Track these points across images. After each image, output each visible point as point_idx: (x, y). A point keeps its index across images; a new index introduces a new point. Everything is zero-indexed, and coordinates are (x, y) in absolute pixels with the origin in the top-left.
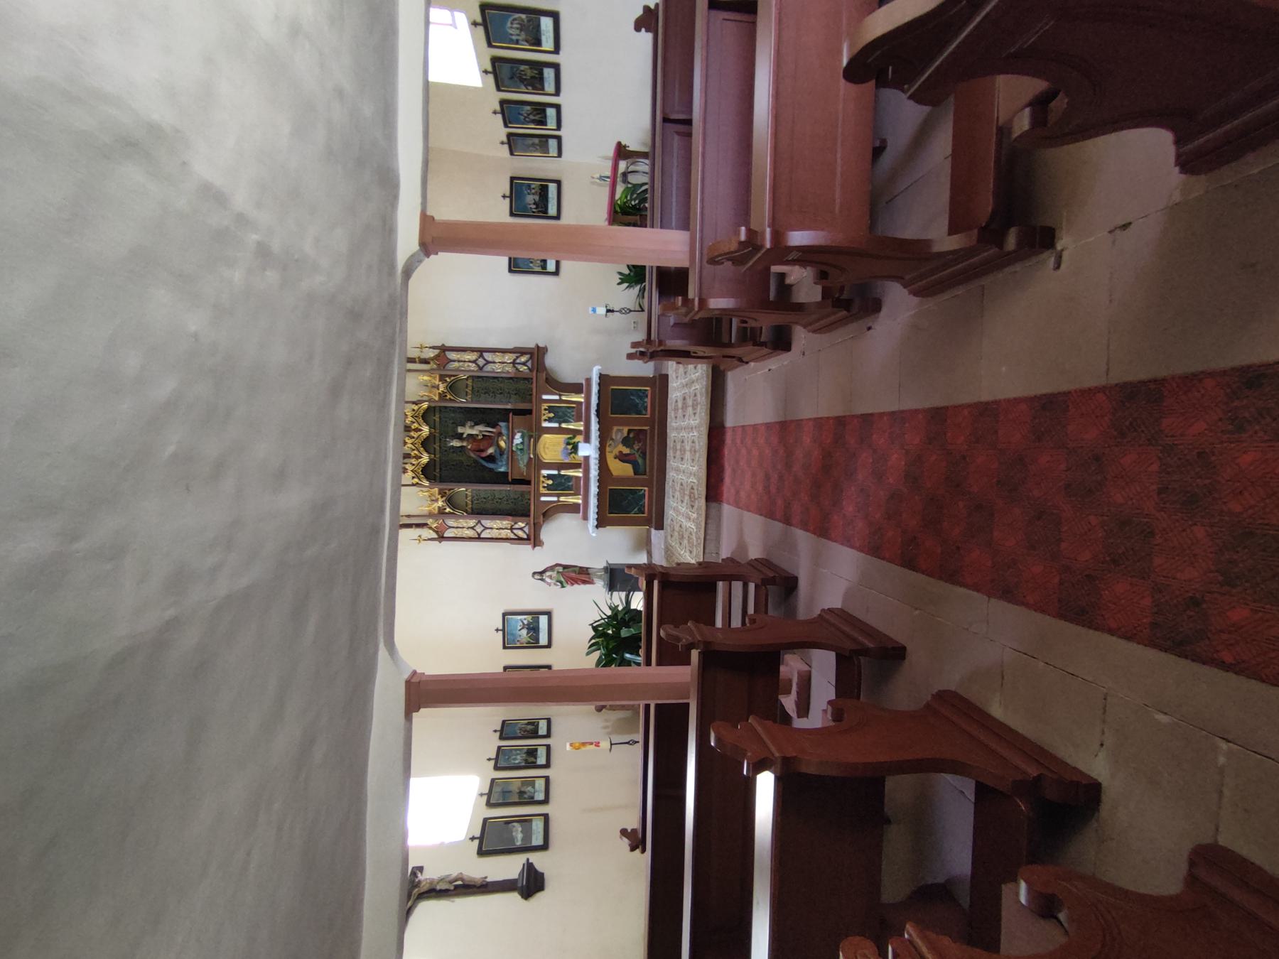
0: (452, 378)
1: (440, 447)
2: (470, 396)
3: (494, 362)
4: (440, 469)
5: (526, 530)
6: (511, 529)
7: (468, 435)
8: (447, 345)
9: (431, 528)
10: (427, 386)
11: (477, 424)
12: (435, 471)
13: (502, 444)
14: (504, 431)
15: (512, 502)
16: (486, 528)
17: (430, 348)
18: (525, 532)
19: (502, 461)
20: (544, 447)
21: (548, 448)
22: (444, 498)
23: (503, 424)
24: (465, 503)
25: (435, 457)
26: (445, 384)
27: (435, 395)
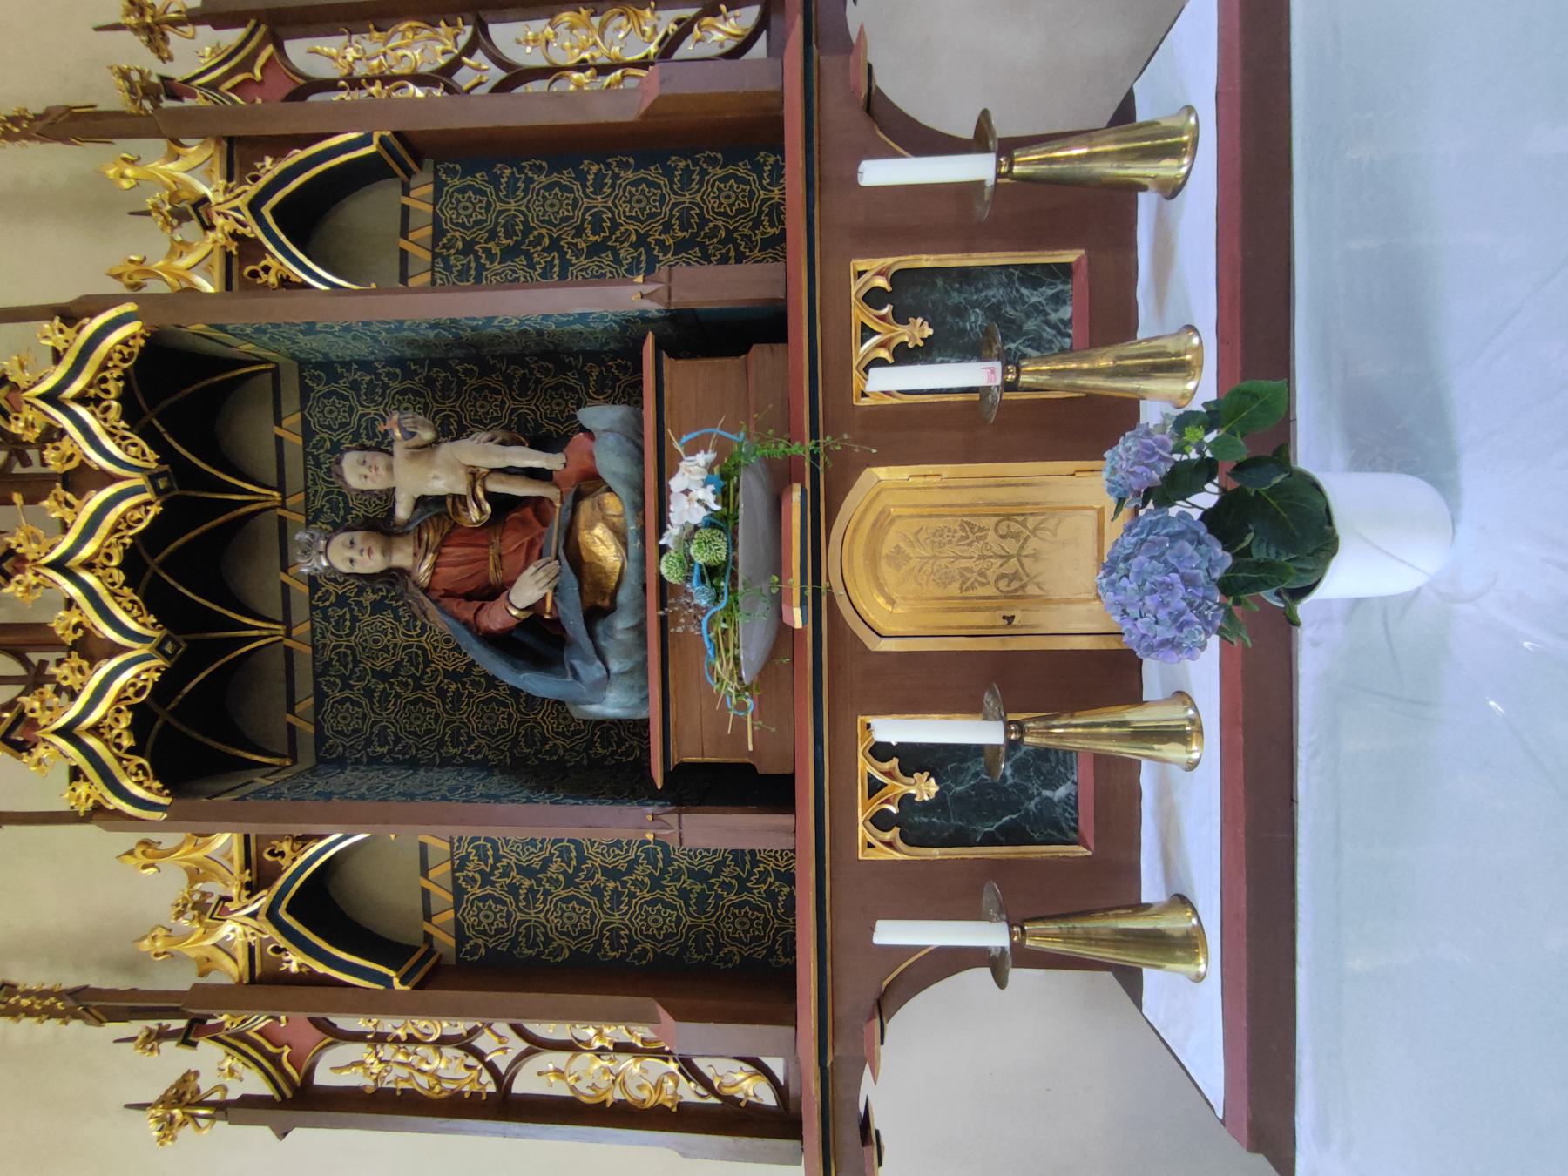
7: (422, 502)
11: (451, 430)
12: (291, 710)
13: (603, 546)
14: (611, 462)
15: (684, 894)
16: (538, 1045)
19: (600, 654)
20: (873, 557)
21: (898, 557)
23: (600, 416)
24: (419, 905)
25: (288, 635)
27: (212, 284)
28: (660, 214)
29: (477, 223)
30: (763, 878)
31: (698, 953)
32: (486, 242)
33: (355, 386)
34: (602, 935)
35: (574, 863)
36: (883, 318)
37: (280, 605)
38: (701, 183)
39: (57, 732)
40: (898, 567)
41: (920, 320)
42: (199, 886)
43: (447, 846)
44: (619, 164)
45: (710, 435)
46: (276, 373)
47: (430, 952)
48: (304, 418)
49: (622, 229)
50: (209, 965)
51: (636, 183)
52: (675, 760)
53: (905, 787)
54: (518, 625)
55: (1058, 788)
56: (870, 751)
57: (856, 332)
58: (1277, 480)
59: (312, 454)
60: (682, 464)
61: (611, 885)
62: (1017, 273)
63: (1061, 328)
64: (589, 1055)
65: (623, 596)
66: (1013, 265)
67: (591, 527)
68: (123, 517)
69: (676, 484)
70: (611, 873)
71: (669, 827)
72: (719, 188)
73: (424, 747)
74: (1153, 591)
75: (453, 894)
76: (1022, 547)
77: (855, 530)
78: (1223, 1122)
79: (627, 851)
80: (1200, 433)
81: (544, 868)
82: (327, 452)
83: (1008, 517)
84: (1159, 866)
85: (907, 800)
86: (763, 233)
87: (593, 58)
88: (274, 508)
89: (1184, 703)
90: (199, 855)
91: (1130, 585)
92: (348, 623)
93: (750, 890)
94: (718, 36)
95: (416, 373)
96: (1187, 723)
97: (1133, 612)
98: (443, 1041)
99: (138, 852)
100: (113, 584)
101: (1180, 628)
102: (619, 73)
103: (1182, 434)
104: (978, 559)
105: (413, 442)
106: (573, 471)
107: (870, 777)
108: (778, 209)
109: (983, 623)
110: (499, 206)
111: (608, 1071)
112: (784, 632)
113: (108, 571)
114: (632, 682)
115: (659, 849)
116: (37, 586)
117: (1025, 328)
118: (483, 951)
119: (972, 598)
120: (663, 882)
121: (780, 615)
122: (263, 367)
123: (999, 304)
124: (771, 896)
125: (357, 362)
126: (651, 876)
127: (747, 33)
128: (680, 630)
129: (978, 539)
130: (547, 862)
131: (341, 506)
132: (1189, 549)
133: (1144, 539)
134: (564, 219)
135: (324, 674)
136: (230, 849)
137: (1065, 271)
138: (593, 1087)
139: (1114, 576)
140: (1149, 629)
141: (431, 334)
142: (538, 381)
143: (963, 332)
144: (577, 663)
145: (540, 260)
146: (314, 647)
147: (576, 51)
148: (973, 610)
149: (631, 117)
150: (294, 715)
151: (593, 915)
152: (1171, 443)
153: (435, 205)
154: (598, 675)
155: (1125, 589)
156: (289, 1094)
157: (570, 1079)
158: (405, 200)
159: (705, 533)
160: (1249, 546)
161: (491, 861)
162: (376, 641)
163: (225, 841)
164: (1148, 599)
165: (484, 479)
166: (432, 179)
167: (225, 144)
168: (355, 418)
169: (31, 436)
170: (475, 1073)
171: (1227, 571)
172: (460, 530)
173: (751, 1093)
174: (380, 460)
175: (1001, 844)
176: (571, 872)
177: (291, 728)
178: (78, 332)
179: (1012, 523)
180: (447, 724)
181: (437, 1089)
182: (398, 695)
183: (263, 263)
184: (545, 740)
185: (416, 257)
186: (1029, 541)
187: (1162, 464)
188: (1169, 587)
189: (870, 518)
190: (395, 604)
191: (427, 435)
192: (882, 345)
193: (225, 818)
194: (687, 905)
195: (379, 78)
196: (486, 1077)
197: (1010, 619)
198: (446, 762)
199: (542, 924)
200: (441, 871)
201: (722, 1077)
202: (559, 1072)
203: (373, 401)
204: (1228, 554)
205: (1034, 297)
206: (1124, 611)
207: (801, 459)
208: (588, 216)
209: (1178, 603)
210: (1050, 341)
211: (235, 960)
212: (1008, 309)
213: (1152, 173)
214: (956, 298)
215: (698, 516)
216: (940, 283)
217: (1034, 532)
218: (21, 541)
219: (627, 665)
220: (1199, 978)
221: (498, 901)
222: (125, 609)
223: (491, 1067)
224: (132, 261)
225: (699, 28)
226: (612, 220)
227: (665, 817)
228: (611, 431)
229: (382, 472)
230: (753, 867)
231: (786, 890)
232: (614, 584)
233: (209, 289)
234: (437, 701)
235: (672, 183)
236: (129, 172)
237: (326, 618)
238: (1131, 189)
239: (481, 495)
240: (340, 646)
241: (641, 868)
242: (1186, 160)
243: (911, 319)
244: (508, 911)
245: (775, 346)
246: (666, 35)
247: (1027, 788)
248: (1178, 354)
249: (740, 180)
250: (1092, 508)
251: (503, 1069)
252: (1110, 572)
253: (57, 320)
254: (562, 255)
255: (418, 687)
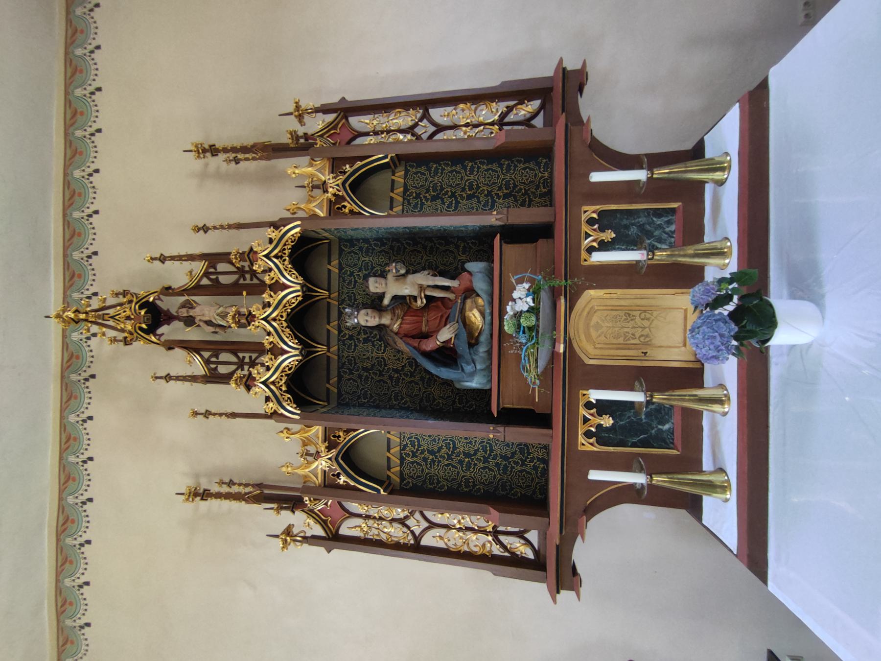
0: (359, 164)
1: (340, 331)
2: (401, 208)
3: (454, 127)
4: (340, 377)
5: (533, 536)
6: (495, 533)
7: (395, 298)
8: (349, 98)
9: (311, 513)
10: (304, 187)
11: (412, 270)
12: (328, 382)
13: (475, 317)
14: (480, 285)
15: (497, 465)
16: (433, 525)
17: (317, 110)
18: (528, 543)
21: (598, 326)
22: (334, 452)
23: (476, 267)
25: (328, 351)
26: (342, 178)
27: (323, 212)
28: (497, 183)
29: (421, 186)
30: (533, 458)
31: (502, 491)
32: (425, 194)
33: (361, 249)
34: (462, 481)
35: (451, 450)
36: (595, 230)
37: (326, 338)
38: (514, 170)
39: (261, 383)
40: (597, 331)
41: (610, 231)
42: (306, 447)
43: (398, 440)
44: (481, 163)
45: (525, 276)
46: (329, 244)
47: (390, 484)
48: (339, 261)
49: (481, 189)
50: (307, 479)
51: (487, 170)
52: (501, 406)
53: (599, 421)
54: (437, 349)
55: (665, 425)
56: (584, 405)
57: (583, 235)
58: (755, 302)
59: (342, 276)
60: (517, 288)
61: (467, 460)
62: (651, 212)
63: (670, 234)
64: (454, 531)
65: (483, 338)
66: (650, 209)
67: (471, 310)
68: (288, 301)
69: (515, 295)
70: (467, 455)
71: (499, 432)
72: (522, 173)
73: (382, 401)
74: (709, 339)
75: (400, 460)
76: (651, 324)
77: (580, 315)
78: (736, 556)
79: (474, 446)
80: (727, 285)
81: (439, 451)
82: (348, 276)
83: (645, 311)
84: (711, 459)
85: (599, 426)
86: (540, 191)
87: (471, 121)
88: (326, 298)
89: (723, 389)
90: (306, 435)
91: (700, 336)
92: (353, 347)
93: (526, 465)
94: (523, 112)
95: (386, 244)
96: (723, 396)
97: (701, 346)
98: (393, 520)
99: (285, 431)
100: (283, 327)
101: (718, 351)
102: (482, 127)
103: (720, 286)
104: (632, 328)
105: (398, 274)
106: (463, 287)
107: (584, 416)
108: (547, 181)
109: (633, 355)
110: (431, 179)
111: (461, 538)
112: (554, 355)
113: (281, 322)
114: (485, 374)
115: (488, 445)
116: (258, 327)
117: (655, 234)
118: (411, 485)
119: (629, 344)
120: (489, 460)
121: (554, 347)
122: (326, 241)
123: (643, 225)
124: (535, 468)
125: (362, 239)
126: (484, 457)
127: (535, 111)
128: (512, 352)
129: (632, 320)
130: (440, 448)
131: (353, 298)
132: (722, 325)
133: (706, 321)
134: (457, 185)
135: (342, 367)
136: (318, 433)
137: (673, 211)
138: (455, 545)
139: (694, 334)
140: (707, 352)
141: (401, 230)
142: (438, 248)
143: (627, 236)
144: (463, 364)
145: (447, 201)
146: (338, 356)
147: (465, 119)
148: (629, 349)
149: (491, 148)
150: (329, 384)
151: (458, 472)
152: (716, 289)
153: (405, 179)
154: (472, 370)
155: (698, 338)
156: (331, 536)
157: (446, 540)
158: (393, 178)
159: (528, 315)
160: (746, 324)
161: (416, 447)
162: (364, 355)
163: (317, 430)
164: (706, 342)
165: (424, 290)
166: (404, 169)
167: (332, 160)
168: (360, 262)
169: (259, 271)
170: (406, 534)
171: (736, 333)
172: (411, 310)
173: (523, 552)
174: (382, 280)
175: (639, 447)
176: (450, 453)
177: (328, 389)
178: (280, 232)
179: (646, 314)
180: (393, 391)
181: (390, 540)
182: (372, 378)
183: (343, 204)
184: (434, 400)
185: (396, 199)
186: (654, 321)
187: (713, 296)
188: (715, 337)
189: (587, 310)
190: (373, 340)
191: (403, 271)
192: (594, 241)
193: (319, 420)
194: (499, 470)
195: (386, 131)
196: (410, 537)
197: (645, 353)
198: (392, 407)
199: (436, 475)
200: (396, 450)
201: (511, 544)
202: (441, 537)
203: (368, 255)
204: (736, 327)
205: (658, 221)
206: (697, 346)
207: (560, 287)
208: (467, 184)
209: (718, 342)
210: (665, 240)
211: (318, 480)
212: (647, 226)
213: (710, 177)
214: (625, 222)
215: (525, 308)
216: (618, 216)
217: (656, 318)
218: (255, 310)
219: (484, 366)
220: (727, 500)
221: (418, 464)
222: (287, 337)
223: (412, 532)
224: (294, 204)
225: (516, 109)
226: (477, 185)
227: (498, 428)
228: (480, 272)
229: (384, 285)
230: (528, 455)
231: (542, 466)
232: (477, 334)
233: (322, 215)
234: (389, 381)
235: (502, 170)
236: (297, 171)
237: (344, 345)
238: (702, 184)
239: (423, 295)
240: (349, 356)
241: (480, 453)
242: (726, 173)
243: (606, 231)
244: (422, 469)
245: (549, 240)
246: (502, 112)
247: (650, 425)
248: (721, 249)
249: (531, 169)
250: (682, 309)
251: (417, 534)
252: (692, 333)
253: (272, 228)
254: (456, 199)
255: (381, 375)
